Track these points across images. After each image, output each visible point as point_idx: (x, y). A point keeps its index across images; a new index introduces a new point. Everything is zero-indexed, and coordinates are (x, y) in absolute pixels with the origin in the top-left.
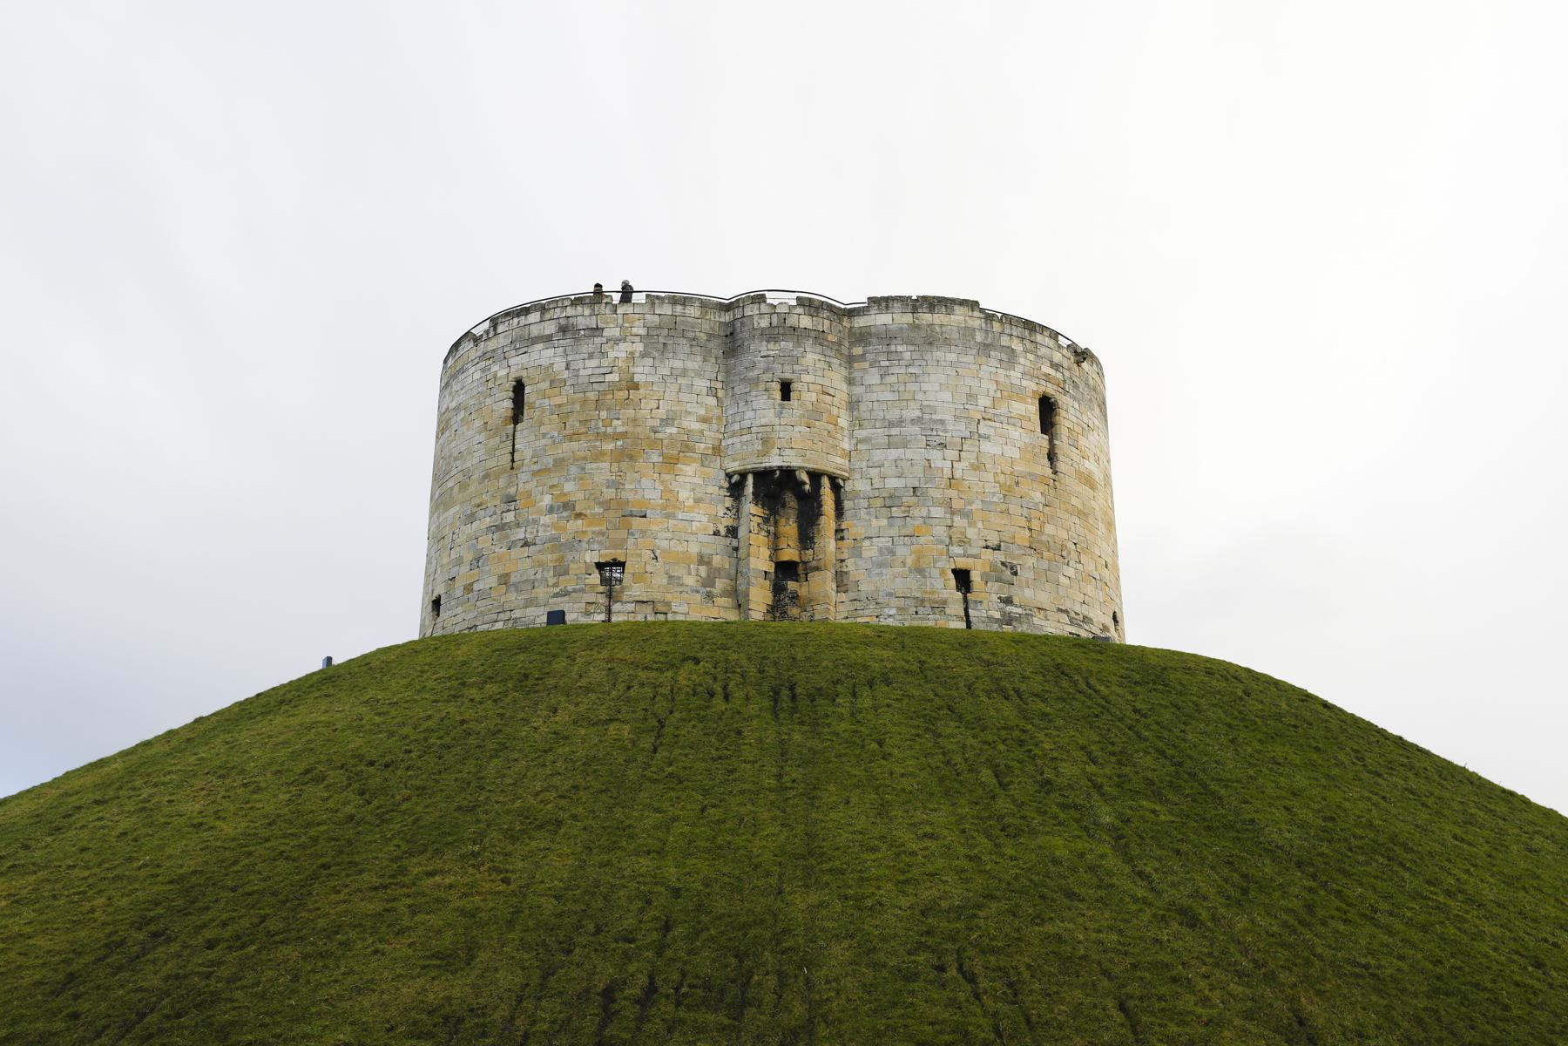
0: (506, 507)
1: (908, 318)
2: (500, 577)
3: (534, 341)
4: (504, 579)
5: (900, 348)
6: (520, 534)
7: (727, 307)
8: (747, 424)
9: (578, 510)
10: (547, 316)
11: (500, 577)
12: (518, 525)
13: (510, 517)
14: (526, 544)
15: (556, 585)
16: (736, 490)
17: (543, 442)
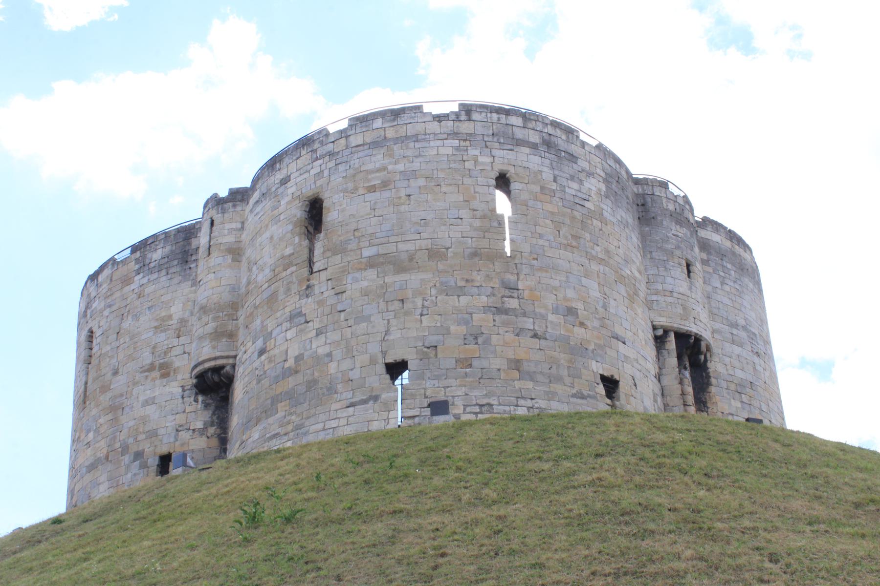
0: (507, 292)
1: (728, 244)
2: (510, 361)
3: (520, 143)
5: (729, 266)
6: (528, 324)
7: (637, 182)
8: (669, 288)
9: (581, 319)
10: (530, 125)
11: (510, 361)
12: (524, 314)
14: (535, 336)
15: (572, 386)
16: (660, 341)
17: (541, 242)
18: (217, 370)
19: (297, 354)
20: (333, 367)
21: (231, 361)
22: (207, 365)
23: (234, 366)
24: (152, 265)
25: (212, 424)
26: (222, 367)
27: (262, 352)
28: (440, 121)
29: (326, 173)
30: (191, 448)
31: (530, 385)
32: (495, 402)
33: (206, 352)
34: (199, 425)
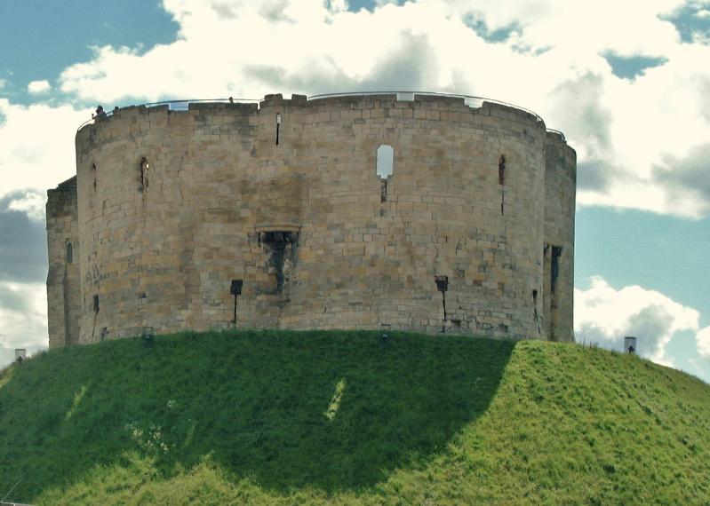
0: (501, 240)
4: (502, 286)
13: (502, 247)
18: (285, 234)
19: (373, 253)
20: (400, 270)
21: (297, 230)
22: (279, 229)
23: (298, 233)
24: (212, 127)
25: (271, 266)
26: (290, 233)
27: (337, 241)
28: (474, 114)
29: (397, 130)
30: (257, 279)
31: (507, 299)
32: (492, 310)
33: (280, 223)
34: (262, 264)
